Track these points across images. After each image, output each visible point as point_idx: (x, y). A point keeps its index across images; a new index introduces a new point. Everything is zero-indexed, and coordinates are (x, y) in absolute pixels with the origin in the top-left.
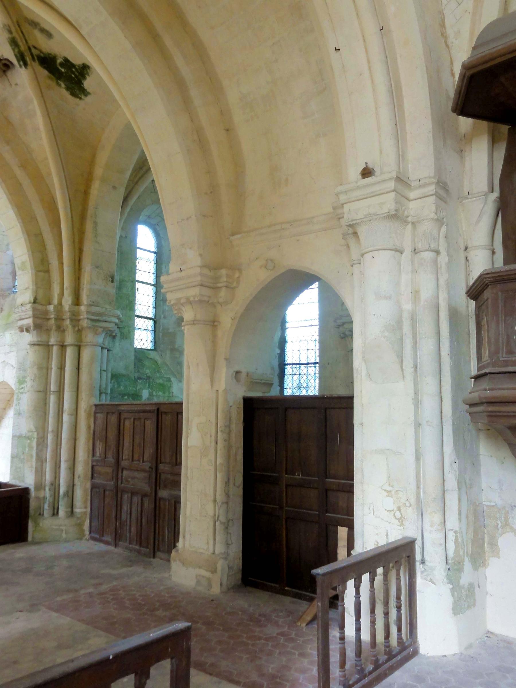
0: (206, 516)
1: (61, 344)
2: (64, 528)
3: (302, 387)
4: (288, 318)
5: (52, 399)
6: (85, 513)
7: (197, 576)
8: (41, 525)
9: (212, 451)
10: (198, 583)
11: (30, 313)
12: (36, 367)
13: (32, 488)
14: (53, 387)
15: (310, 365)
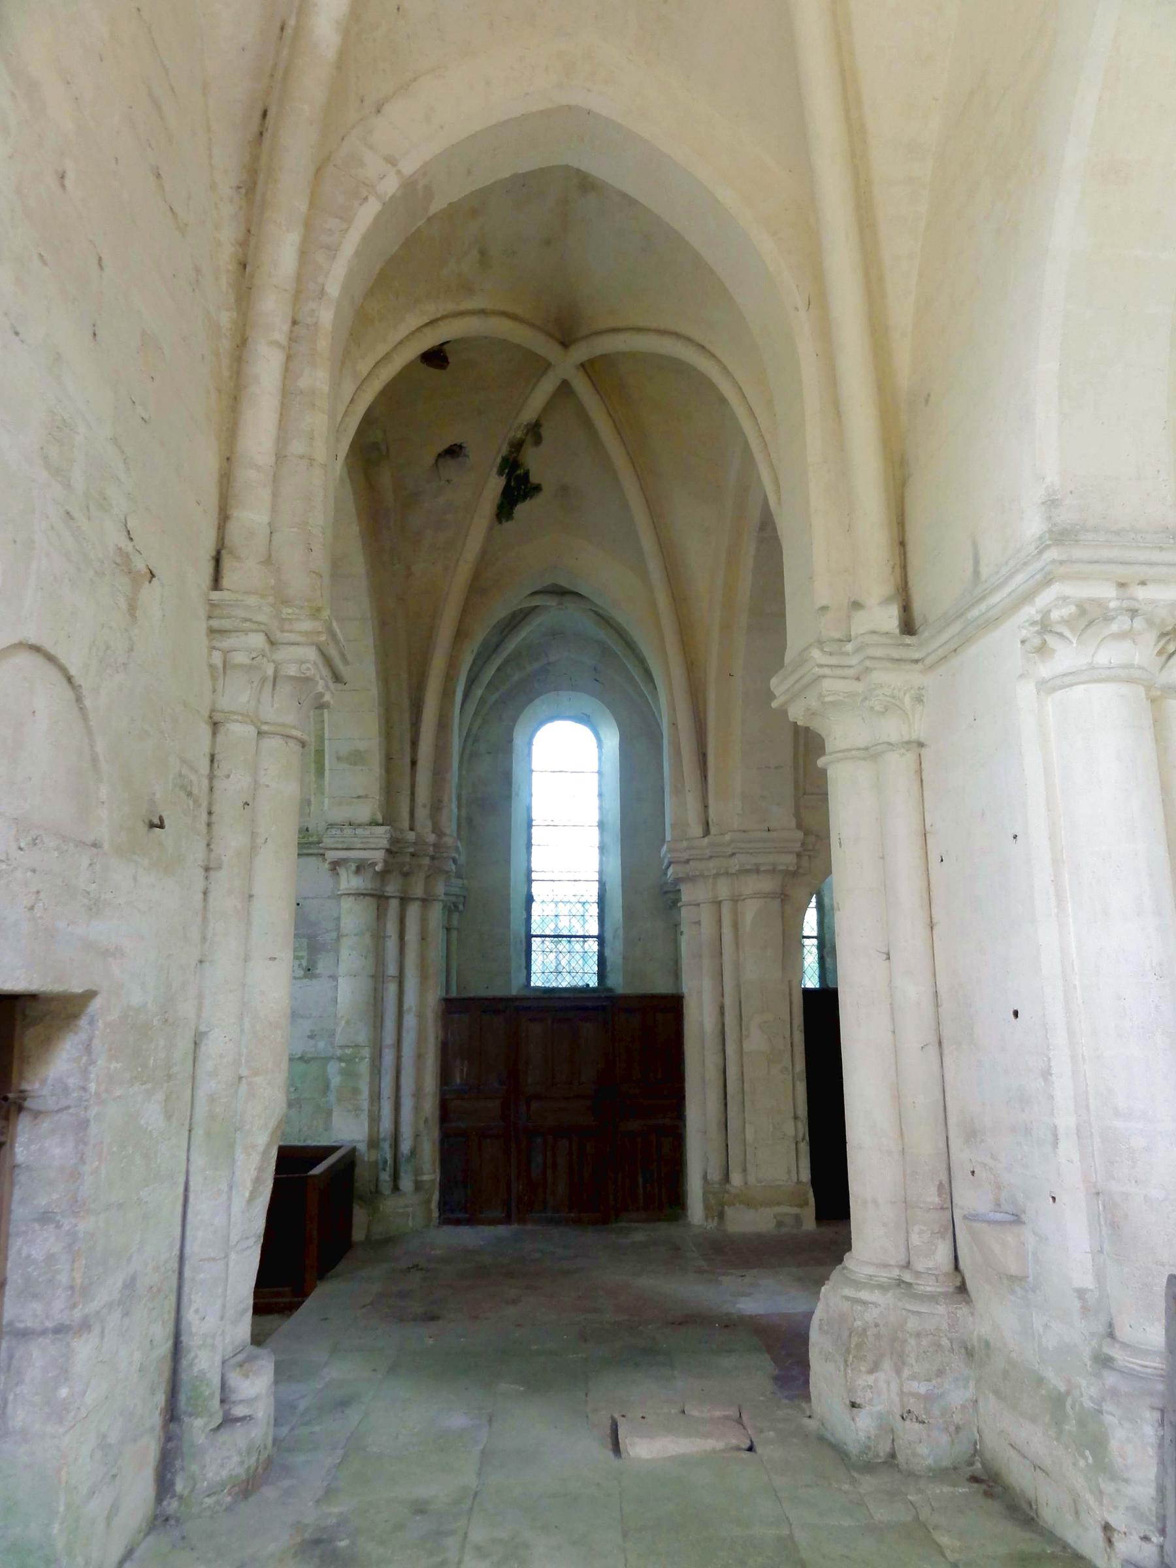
0: (783, 1138)
1: (403, 895)
2: (410, 1210)
3: (564, 970)
4: (535, 865)
5: (392, 988)
6: (433, 1181)
7: (775, 1217)
8: (381, 1209)
9: (787, 1056)
10: (780, 1224)
11: (384, 843)
12: (368, 935)
13: (362, 1147)
14: (392, 970)
15: (578, 939)
